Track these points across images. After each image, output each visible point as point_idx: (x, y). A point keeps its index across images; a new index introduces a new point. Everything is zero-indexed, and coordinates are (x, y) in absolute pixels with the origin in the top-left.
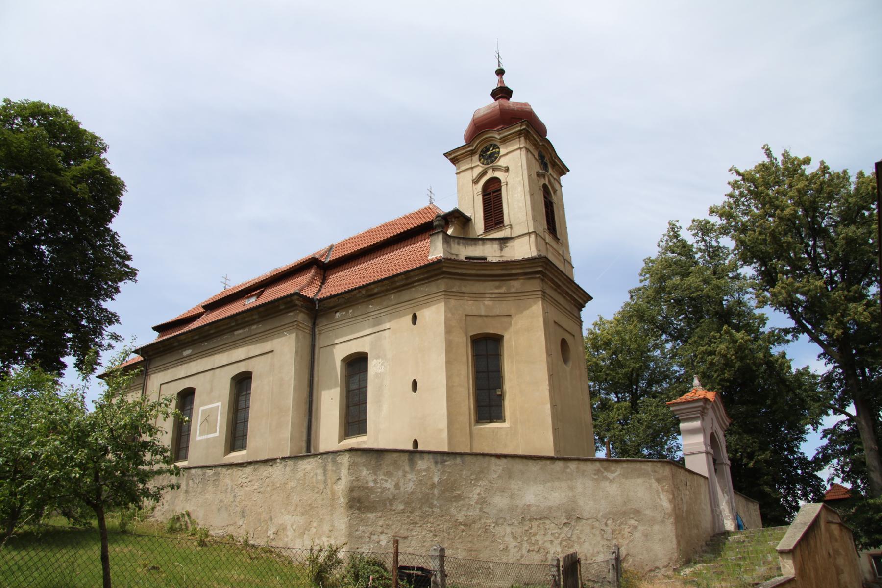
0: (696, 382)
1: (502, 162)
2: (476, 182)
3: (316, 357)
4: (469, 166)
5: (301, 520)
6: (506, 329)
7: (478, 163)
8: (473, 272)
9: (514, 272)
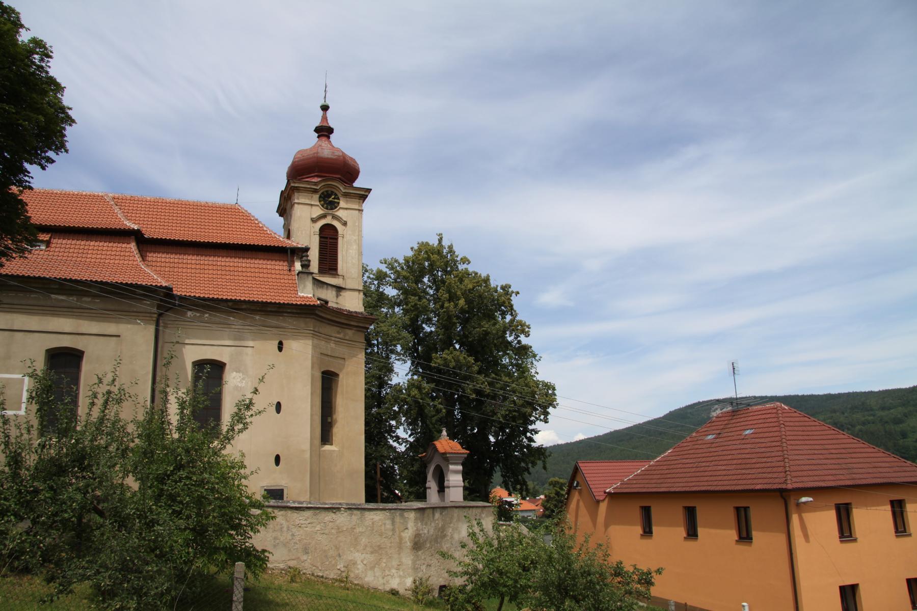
0: (444, 433)
1: (340, 213)
2: (314, 221)
3: (159, 349)
4: (308, 201)
5: (372, 558)
6: (341, 370)
7: (318, 203)
8: (329, 317)
9: (352, 323)
